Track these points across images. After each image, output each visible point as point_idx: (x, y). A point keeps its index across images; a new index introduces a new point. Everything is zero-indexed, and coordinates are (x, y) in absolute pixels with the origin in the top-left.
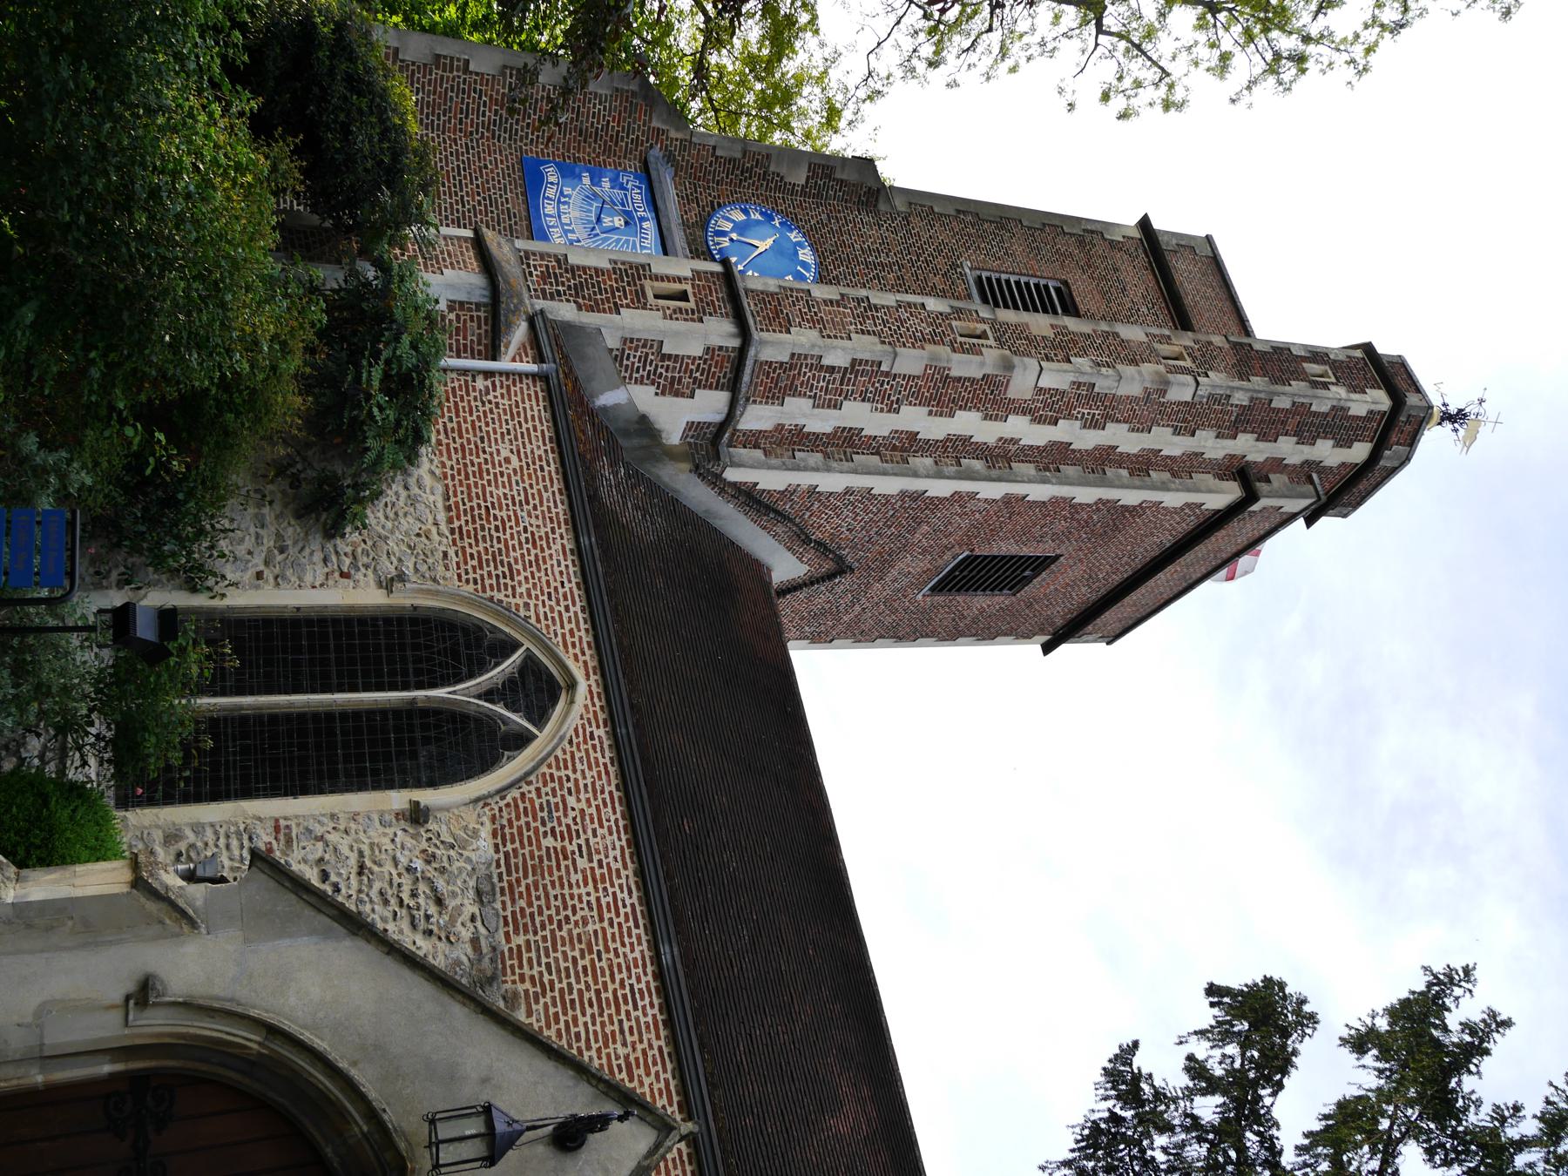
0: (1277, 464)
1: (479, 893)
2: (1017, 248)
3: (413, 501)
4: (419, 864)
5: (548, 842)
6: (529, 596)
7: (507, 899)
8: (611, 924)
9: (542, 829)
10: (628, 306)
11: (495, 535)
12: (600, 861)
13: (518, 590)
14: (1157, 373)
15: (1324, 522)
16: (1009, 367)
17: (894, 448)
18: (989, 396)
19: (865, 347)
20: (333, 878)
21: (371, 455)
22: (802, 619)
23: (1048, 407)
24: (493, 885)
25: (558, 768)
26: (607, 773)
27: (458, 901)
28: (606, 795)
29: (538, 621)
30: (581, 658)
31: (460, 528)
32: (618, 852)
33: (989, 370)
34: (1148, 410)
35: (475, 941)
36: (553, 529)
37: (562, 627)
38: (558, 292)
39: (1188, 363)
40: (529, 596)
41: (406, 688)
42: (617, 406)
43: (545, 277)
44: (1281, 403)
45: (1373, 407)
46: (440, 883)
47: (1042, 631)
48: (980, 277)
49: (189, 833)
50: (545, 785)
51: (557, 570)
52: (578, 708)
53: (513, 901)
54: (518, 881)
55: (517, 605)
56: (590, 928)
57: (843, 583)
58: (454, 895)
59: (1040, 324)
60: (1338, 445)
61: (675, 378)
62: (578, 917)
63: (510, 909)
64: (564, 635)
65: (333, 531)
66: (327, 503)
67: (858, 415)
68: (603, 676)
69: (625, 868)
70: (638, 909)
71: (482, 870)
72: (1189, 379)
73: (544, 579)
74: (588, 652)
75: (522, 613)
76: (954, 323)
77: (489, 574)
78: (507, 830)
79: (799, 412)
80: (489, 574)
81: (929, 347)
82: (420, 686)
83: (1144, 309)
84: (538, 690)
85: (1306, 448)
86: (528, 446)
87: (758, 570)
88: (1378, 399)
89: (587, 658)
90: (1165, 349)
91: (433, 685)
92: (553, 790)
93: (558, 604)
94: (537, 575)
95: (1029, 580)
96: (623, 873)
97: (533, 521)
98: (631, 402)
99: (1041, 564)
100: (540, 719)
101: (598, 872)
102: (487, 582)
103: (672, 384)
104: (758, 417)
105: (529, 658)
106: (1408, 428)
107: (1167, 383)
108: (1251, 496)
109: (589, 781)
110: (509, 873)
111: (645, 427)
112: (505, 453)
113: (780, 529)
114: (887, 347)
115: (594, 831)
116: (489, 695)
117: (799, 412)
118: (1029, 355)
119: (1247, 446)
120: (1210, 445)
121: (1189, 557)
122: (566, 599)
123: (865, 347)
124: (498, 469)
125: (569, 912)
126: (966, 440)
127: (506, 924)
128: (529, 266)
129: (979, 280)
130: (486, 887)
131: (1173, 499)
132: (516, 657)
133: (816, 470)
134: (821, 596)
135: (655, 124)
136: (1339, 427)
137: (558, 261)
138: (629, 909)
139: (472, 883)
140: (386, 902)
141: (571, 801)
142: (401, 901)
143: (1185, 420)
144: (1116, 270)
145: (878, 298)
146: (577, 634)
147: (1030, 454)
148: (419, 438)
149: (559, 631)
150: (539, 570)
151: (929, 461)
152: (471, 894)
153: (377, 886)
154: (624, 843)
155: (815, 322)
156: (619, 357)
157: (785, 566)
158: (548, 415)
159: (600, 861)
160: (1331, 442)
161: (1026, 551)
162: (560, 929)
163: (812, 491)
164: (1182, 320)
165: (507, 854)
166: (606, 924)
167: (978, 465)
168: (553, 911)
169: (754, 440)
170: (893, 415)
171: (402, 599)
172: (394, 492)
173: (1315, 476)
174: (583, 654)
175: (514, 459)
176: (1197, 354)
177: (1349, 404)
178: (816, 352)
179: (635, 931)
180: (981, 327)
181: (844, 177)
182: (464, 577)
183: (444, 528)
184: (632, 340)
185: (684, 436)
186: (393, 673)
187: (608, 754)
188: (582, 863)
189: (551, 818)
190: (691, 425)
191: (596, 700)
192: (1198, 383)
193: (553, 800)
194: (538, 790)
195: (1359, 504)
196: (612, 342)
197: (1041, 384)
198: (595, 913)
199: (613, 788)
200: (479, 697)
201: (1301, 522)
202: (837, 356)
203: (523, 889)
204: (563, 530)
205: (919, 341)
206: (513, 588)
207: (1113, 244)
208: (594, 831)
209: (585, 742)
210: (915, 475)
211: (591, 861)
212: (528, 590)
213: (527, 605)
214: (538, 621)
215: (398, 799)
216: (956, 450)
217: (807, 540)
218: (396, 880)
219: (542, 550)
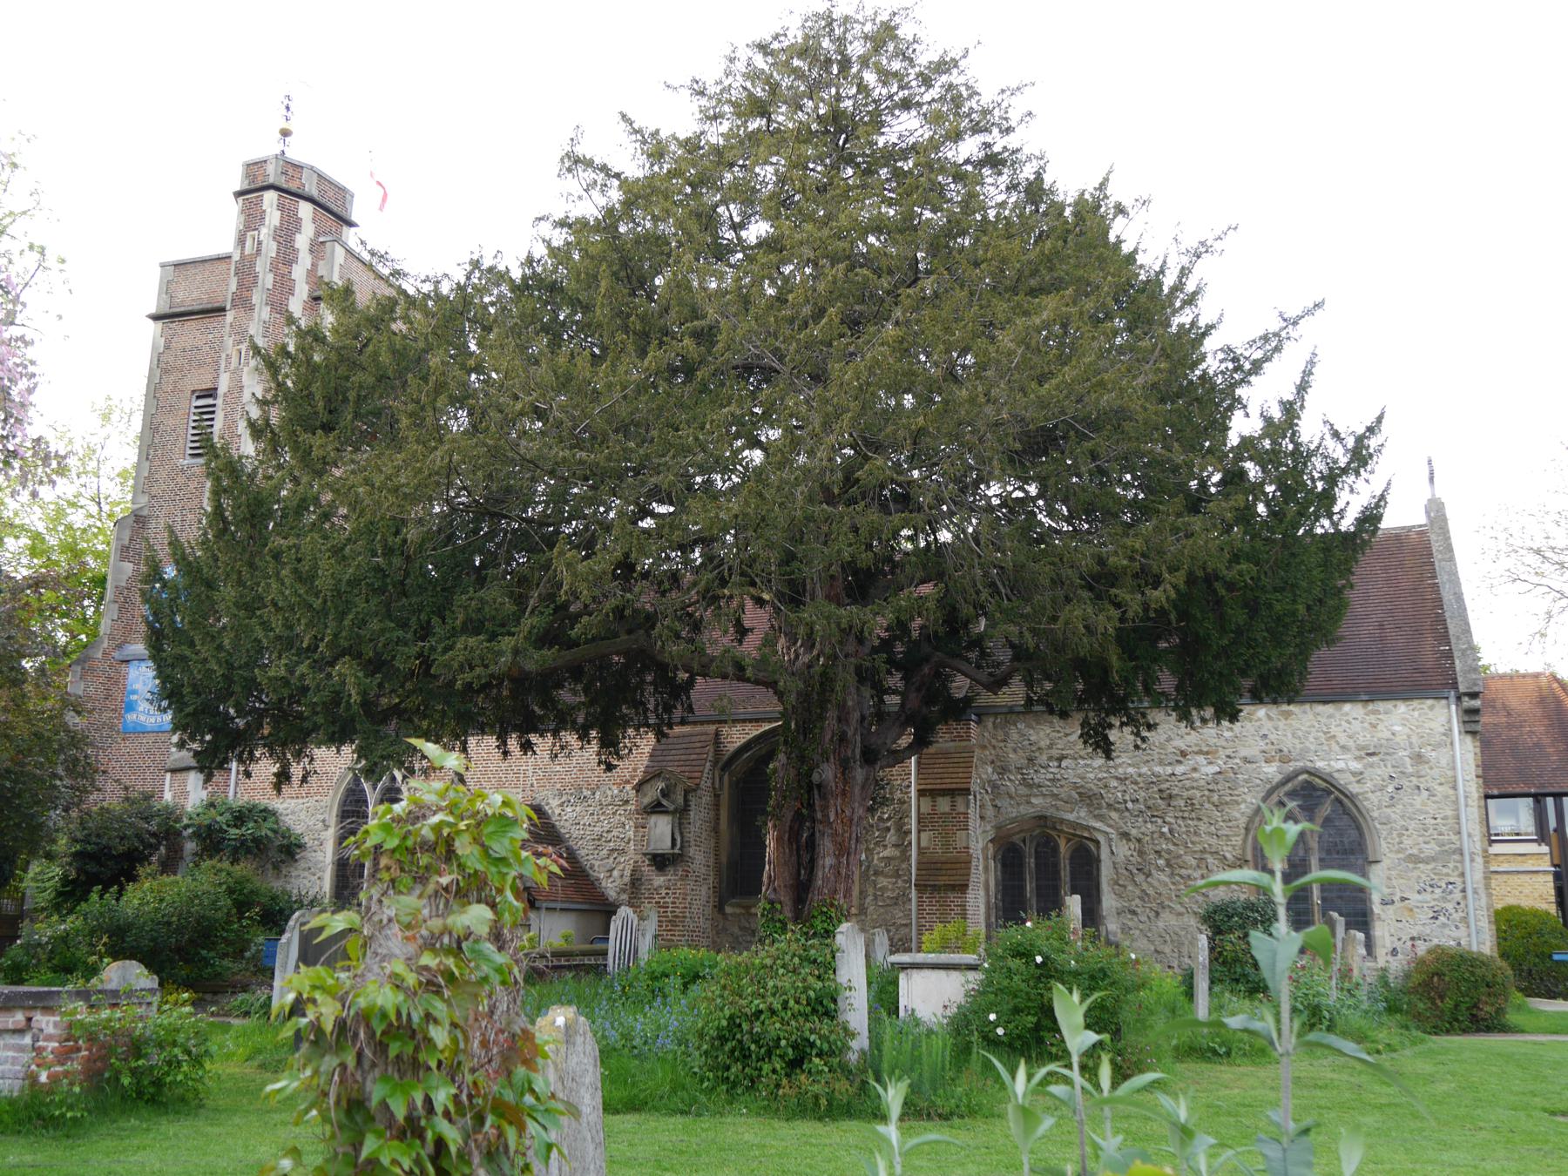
0: (312, 272)
3: (293, 813)
21: (270, 834)
44: (268, 280)
65: (301, 846)
66: (290, 850)
85: (301, 255)
135: (100, 655)
136: (289, 228)
148: (265, 810)
172: (289, 821)
207: (167, 347)
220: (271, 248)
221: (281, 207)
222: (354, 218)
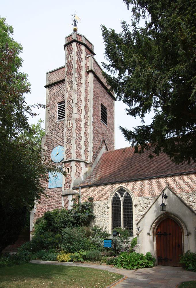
0: (86, 65)
4: (141, 205)
5: (140, 190)
16: (74, 119)
17: (87, 136)
18: (78, 121)
19: (73, 142)
22: (111, 145)
23: (79, 111)
33: (75, 122)
34: (79, 92)
35: (151, 200)
42: (83, 178)
44: (75, 66)
45: (75, 46)
46: (144, 203)
48: (58, 119)
57: (106, 140)
59: (67, 112)
60: (82, 53)
61: (79, 170)
67: (82, 143)
79: (82, 151)
81: (72, 132)
82: (121, 204)
87: (104, 155)
88: (74, 44)
91: (120, 203)
95: (105, 107)
99: (102, 106)
100: (125, 191)
105: (117, 191)
106: (78, 37)
111: (86, 173)
116: (122, 197)
117: (82, 151)
119: (83, 73)
123: (73, 142)
132: (118, 193)
134: (107, 142)
136: (79, 53)
139: (144, 200)
141: (135, 187)
145: (65, 139)
147: (86, 113)
156: (77, 177)
161: (101, 110)
165: (141, 195)
169: (86, 158)
171: (110, 206)
173: (87, 56)
175: (92, 192)
176: (69, 83)
177: (75, 52)
178: (74, 149)
180: (68, 123)
183: (101, 201)
192: (74, 84)
196: (75, 179)
201: (95, 57)
202: (74, 146)
205: (71, 133)
213: (111, 192)
215: (134, 207)
216: (86, 125)
220: (75, 57)
221: (77, 46)
222: (95, 52)
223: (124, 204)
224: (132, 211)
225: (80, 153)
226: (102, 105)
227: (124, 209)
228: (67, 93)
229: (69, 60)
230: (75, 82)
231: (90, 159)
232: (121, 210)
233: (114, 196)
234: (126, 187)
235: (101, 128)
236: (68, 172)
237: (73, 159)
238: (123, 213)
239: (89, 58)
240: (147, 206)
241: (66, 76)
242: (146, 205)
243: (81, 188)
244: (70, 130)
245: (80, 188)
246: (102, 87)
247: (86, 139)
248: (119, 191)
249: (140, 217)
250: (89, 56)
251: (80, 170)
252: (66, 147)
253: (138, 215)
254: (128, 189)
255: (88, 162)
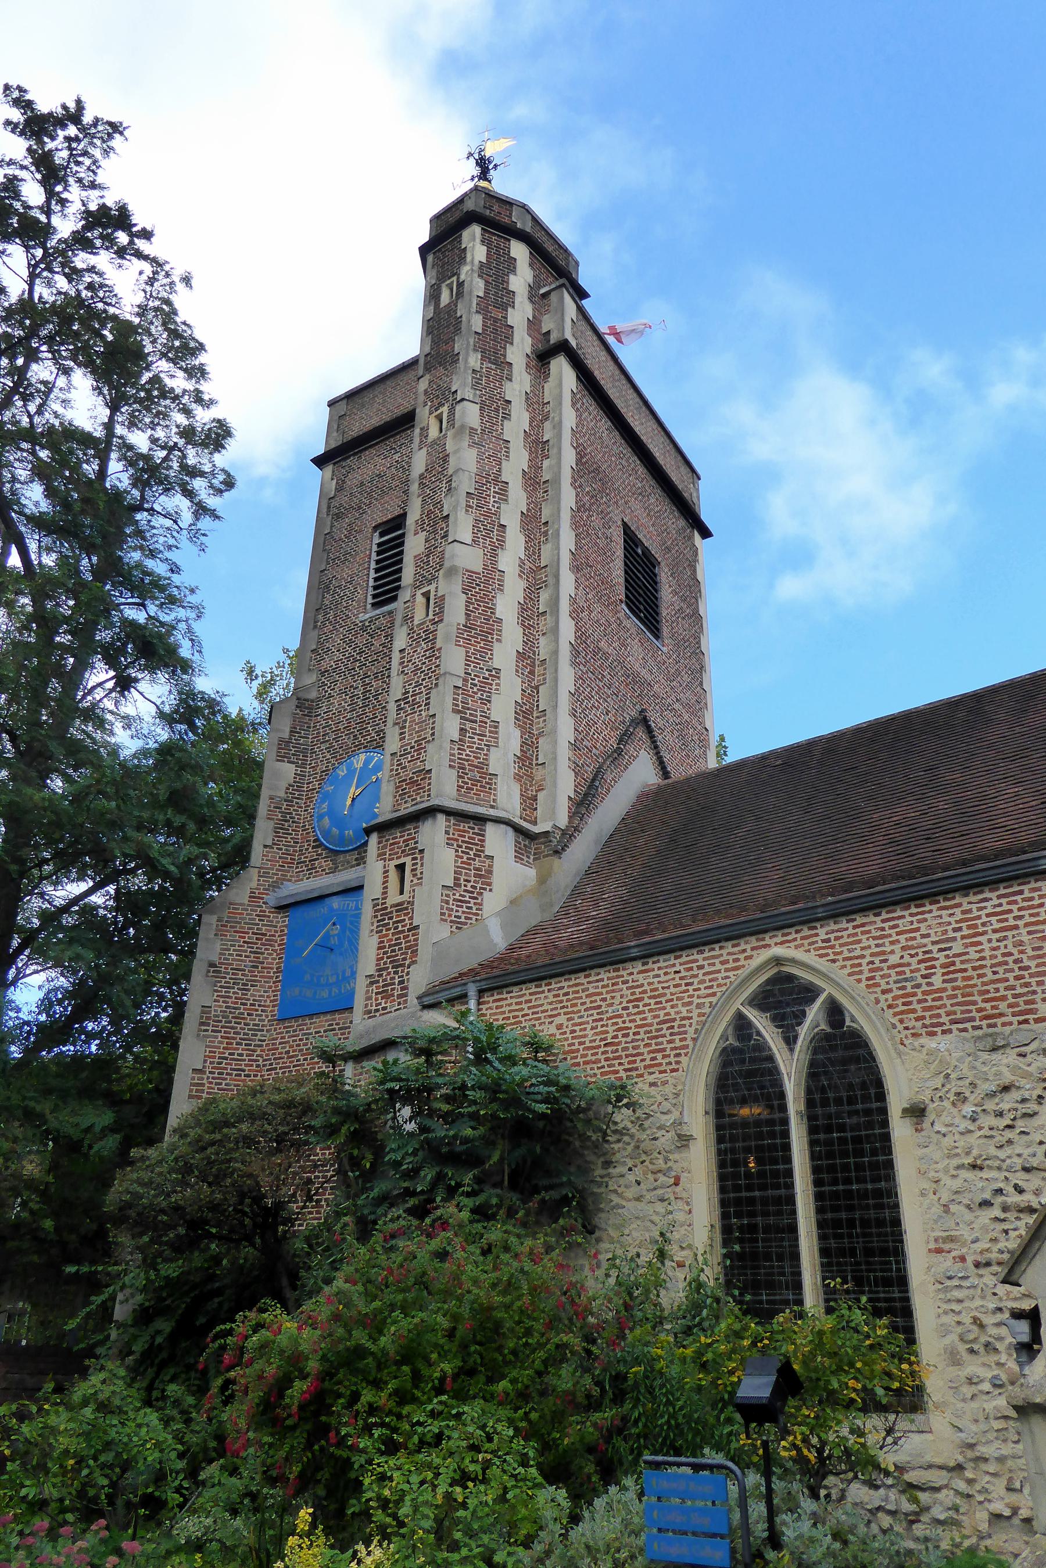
0: (533, 324)
1: (994, 1049)
2: (346, 573)
4: (968, 1109)
5: (937, 981)
6: (690, 1003)
7: (999, 1021)
8: (1021, 917)
9: (925, 988)
10: (411, 918)
11: (631, 1037)
12: (955, 930)
13: (684, 1014)
14: (455, 437)
15: (583, 282)
17: (532, 672)
18: (482, 587)
19: (443, 700)
20: (987, 1195)
23: (489, 532)
24: (987, 1035)
25: (861, 972)
26: (863, 925)
27: (1005, 1070)
28: (886, 925)
29: (714, 994)
30: (749, 953)
31: (625, 1070)
32: (944, 913)
36: (624, 983)
37: (719, 971)
38: (401, 982)
39: (445, 410)
40: (690, 1003)
41: (785, 1122)
42: (503, 926)
43: (386, 995)
44: (477, 323)
47: (691, 538)
48: (373, 605)
49: (947, 1340)
50: (878, 985)
51: (663, 978)
52: (799, 955)
53: (1001, 1015)
54: (979, 1010)
55: (700, 1015)
56: (1026, 938)
58: (998, 1074)
59: (414, 545)
60: (514, 271)
61: (476, 875)
62: (1015, 951)
63: (1010, 1019)
64: (726, 970)
67: (503, 706)
68: (765, 931)
69: (960, 905)
70: (1002, 891)
71: (969, 1047)
72: (458, 408)
73: (673, 990)
74: (743, 947)
75: (707, 1010)
76: (416, 622)
77: (669, 1042)
78: (927, 1022)
80: (669, 1042)
82: (783, 1108)
83: (396, 457)
84: (784, 996)
85: (518, 300)
86: (545, 1008)
89: (748, 947)
90: (433, 432)
91: (782, 1095)
92: (882, 977)
93: (696, 976)
94: (669, 997)
95: (646, 552)
96: (966, 907)
97: (617, 1001)
98: (498, 914)
99: (631, 539)
100: (809, 993)
101: (965, 932)
102: (678, 1044)
103: (480, 876)
104: (508, 799)
106: (496, 208)
107: (463, 427)
108: (563, 348)
109: (872, 943)
110: (973, 1019)
112: (553, 1030)
113: (609, 776)
114: (441, 681)
115: (923, 936)
116: (790, 1041)
118: (443, 552)
120: (518, 385)
121: (620, 404)
122: (691, 969)
124: (568, 1035)
125: (1010, 959)
126: (523, 608)
127: (1026, 1021)
128: (377, 1011)
129: (375, 605)
130: (989, 1043)
131: (569, 418)
132: (753, 1015)
133: (555, 743)
134: (666, 739)
137: (372, 983)
138: (1004, 901)
139: (985, 1056)
140: (1010, 1142)
141: (894, 959)
142: (1008, 1127)
143: (497, 410)
144: (362, 484)
145: (397, 691)
146: (725, 957)
147: (533, 550)
149: (723, 974)
150: (665, 995)
151: (543, 641)
152: (996, 1056)
153: (993, 1151)
154: (934, 907)
155: (420, 747)
156: (459, 925)
157: (640, 773)
158: (515, 989)
159: (955, 930)
160: (512, 277)
161: (620, 552)
162: (1028, 968)
163: (575, 746)
164: (406, 421)
165: (954, 1022)
166: (1020, 923)
167: (544, 596)
168: (1010, 976)
169: (529, 802)
170: (502, 674)
171: (699, 1123)
173: (542, 291)
174: (744, 951)
175: (558, 1020)
177: (476, 262)
179: (1027, 894)
180: (420, 599)
181: (288, 730)
182: (674, 1066)
184: (442, 914)
185: (528, 865)
186: (772, 1135)
187: (844, 925)
188: (957, 948)
189: (912, 979)
190: (518, 858)
191: (789, 938)
192: (463, 400)
193: (894, 978)
194: (884, 992)
195: (566, 250)
196: (443, 931)
197: (469, 541)
198: (1009, 934)
199: (878, 919)
200: (792, 1050)
201: (585, 303)
202: (451, 726)
203: (988, 1006)
204: (624, 973)
205: (434, 653)
206: (683, 1019)
207: (340, 489)
208: (923, 936)
209: (832, 947)
210: (556, 652)
211: (954, 939)
212: (684, 1005)
213: (699, 1006)
214: (714, 994)
215: (900, 1129)
216: (529, 614)
217: (619, 752)
218: (986, 1132)
219: (645, 992)
220: (478, 287)
223: (810, 1103)
224: (890, 1164)
225: (482, 767)
226: (625, 533)
227: (812, 1143)
228: (425, 450)
229: (442, 305)
230: (469, 394)
231: (554, 813)
232: (788, 1160)
233: (724, 1037)
234: (821, 964)
235: (625, 646)
236: (402, 892)
237: (435, 802)
238: (811, 1187)
239: (554, 297)
240: (1025, 1115)
241: (421, 373)
242: (1007, 1103)
243: (481, 992)
244: (430, 637)
245: (472, 990)
246: (625, 445)
247: (531, 692)
248: (763, 1000)
249: (968, 1216)
250: (553, 286)
251: (485, 876)
252: (397, 737)
253: (945, 1197)
254: (841, 975)
255: (536, 829)
